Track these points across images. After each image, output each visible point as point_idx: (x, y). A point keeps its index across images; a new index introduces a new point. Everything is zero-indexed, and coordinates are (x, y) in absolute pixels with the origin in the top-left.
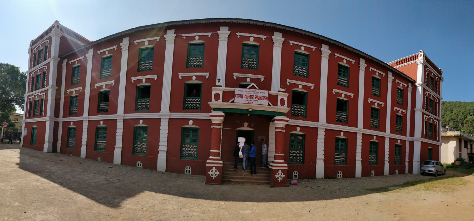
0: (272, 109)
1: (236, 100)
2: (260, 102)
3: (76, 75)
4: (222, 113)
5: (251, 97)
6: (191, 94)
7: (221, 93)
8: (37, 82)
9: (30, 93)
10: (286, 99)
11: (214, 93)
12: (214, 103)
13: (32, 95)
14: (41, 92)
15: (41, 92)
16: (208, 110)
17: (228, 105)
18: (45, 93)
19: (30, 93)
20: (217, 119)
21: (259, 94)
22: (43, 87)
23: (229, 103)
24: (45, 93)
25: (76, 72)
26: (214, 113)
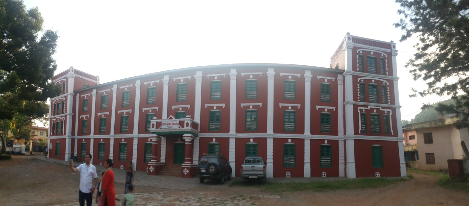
9: (53, 117)
13: (55, 118)
14: (61, 117)
15: (61, 117)
19: (53, 117)
22: (63, 113)
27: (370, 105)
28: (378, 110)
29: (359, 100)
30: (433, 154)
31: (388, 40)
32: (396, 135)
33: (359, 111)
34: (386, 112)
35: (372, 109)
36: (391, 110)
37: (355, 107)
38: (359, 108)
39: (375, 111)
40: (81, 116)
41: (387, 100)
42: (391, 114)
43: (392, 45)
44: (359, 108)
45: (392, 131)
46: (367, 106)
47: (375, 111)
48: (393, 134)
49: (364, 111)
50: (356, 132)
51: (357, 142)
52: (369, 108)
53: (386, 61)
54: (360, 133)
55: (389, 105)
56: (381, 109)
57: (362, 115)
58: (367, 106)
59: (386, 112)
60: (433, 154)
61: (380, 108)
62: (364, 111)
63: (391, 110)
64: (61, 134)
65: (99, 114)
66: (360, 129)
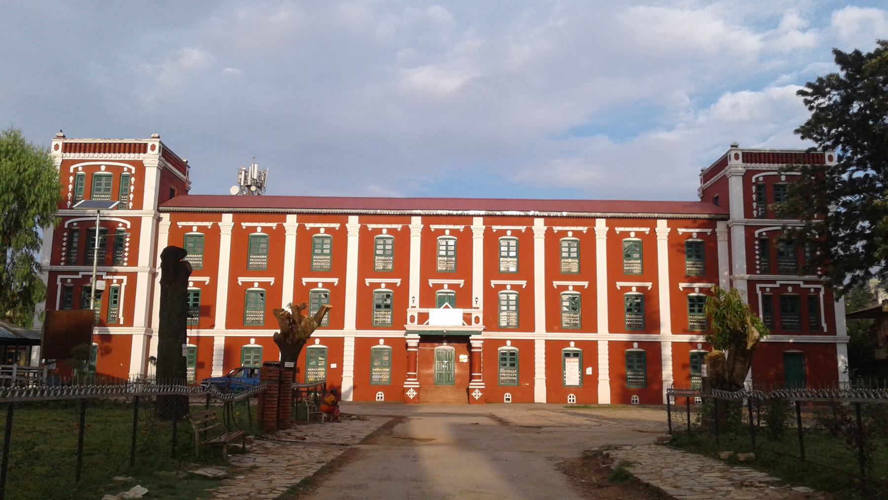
0: (467, 328)
10: (481, 316)
12: (410, 326)
17: (423, 328)
20: (413, 342)
28: (796, 287)
29: (758, 272)
32: (832, 330)
33: (759, 292)
34: (812, 290)
35: (784, 287)
38: (758, 286)
39: (790, 289)
44: (758, 286)
45: (824, 325)
46: (774, 282)
47: (790, 289)
48: (825, 330)
49: (768, 290)
56: (802, 286)
58: (774, 282)
59: (812, 290)
61: (801, 283)
62: (768, 290)
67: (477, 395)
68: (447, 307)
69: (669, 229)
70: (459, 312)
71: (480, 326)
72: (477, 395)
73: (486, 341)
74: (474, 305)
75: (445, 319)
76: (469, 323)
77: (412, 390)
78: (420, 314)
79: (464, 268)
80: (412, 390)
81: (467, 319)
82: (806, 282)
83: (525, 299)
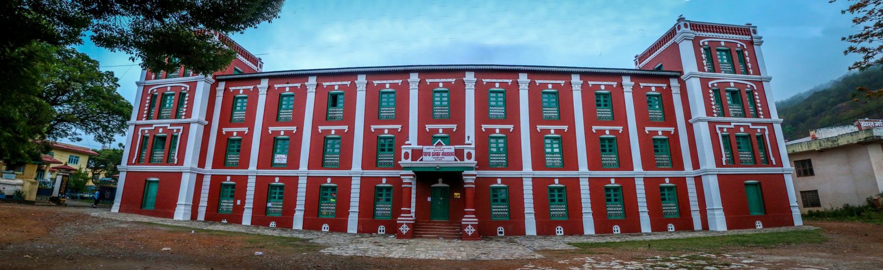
1: (425, 158)
2: (447, 158)
3: (238, 108)
4: (410, 172)
5: (438, 154)
6: (379, 149)
7: (410, 152)
8: (162, 104)
10: (473, 152)
11: (403, 151)
12: (403, 162)
16: (398, 167)
18: (181, 128)
20: (408, 178)
21: (445, 151)
23: (418, 162)
24: (181, 128)
25: (239, 104)
26: (404, 172)
27: (735, 121)
28: (747, 128)
30: (816, 191)
31: (741, 23)
33: (719, 132)
34: (759, 131)
35: (737, 128)
36: (766, 127)
37: (712, 125)
38: (717, 126)
39: (742, 129)
40: (225, 130)
41: (757, 111)
42: (767, 133)
43: (751, 29)
44: (717, 126)
45: (773, 159)
47: (742, 129)
49: (725, 130)
50: (719, 163)
51: (722, 179)
52: (732, 126)
53: (746, 53)
54: (724, 164)
55: (762, 119)
56: (751, 127)
57: (723, 136)
58: (729, 123)
59: (759, 131)
60: (816, 191)
62: (725, 130)
63: (766, 127)
64: (168, 161)
65: (271, 129)
66: (724, 159)
67: (470, 231)
68: (439, 144)
69: (633, 83)
70: (452, 149)
71: (473, 161)
72: (470, 231)
73: (478, 180)
74: (467, 142)
75: (439, 157)
76: (462, 159)
77: (404, 226)
78: (413, 150)
79: (457, 114)
80: (404, 226)
81: (459, 154)
82: (753, 124)
83: (512, 141)
